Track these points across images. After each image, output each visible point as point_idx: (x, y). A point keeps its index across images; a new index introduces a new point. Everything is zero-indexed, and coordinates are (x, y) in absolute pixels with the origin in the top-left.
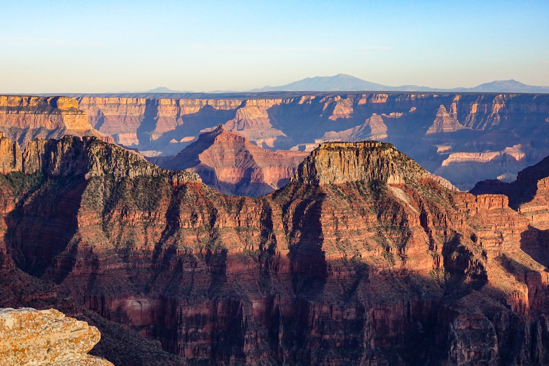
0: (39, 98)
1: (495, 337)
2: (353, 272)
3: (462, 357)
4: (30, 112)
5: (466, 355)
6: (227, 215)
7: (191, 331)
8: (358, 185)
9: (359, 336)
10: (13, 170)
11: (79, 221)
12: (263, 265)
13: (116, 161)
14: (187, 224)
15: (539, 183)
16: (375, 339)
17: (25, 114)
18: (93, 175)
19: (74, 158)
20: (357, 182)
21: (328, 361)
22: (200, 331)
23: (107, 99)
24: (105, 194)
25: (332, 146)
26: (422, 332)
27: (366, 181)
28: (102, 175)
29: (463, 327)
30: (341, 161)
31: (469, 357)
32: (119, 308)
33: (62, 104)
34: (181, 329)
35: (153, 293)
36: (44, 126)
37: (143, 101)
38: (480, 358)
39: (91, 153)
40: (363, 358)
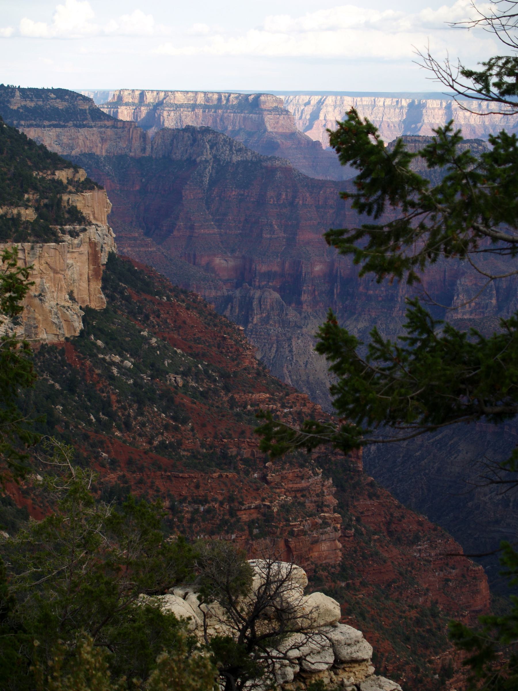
0: (240, 94)
1: (494, 292)
4: (229, 111)
6: (308, 195)
7: (263, 283)
11: (183, 194)
13: (222, 147)
14: (272, 200)
18: (203, 159)
19: (192, 145)
21: (369, 311)
22: (270, 284)
23: (359, 99)
24: (211, 174)
32: (208, 264)
33: (265, 102)
34: (255, 281)
35: (237, 254)
36: (243, 127)
37: (405, 103)
39: (203, 140)
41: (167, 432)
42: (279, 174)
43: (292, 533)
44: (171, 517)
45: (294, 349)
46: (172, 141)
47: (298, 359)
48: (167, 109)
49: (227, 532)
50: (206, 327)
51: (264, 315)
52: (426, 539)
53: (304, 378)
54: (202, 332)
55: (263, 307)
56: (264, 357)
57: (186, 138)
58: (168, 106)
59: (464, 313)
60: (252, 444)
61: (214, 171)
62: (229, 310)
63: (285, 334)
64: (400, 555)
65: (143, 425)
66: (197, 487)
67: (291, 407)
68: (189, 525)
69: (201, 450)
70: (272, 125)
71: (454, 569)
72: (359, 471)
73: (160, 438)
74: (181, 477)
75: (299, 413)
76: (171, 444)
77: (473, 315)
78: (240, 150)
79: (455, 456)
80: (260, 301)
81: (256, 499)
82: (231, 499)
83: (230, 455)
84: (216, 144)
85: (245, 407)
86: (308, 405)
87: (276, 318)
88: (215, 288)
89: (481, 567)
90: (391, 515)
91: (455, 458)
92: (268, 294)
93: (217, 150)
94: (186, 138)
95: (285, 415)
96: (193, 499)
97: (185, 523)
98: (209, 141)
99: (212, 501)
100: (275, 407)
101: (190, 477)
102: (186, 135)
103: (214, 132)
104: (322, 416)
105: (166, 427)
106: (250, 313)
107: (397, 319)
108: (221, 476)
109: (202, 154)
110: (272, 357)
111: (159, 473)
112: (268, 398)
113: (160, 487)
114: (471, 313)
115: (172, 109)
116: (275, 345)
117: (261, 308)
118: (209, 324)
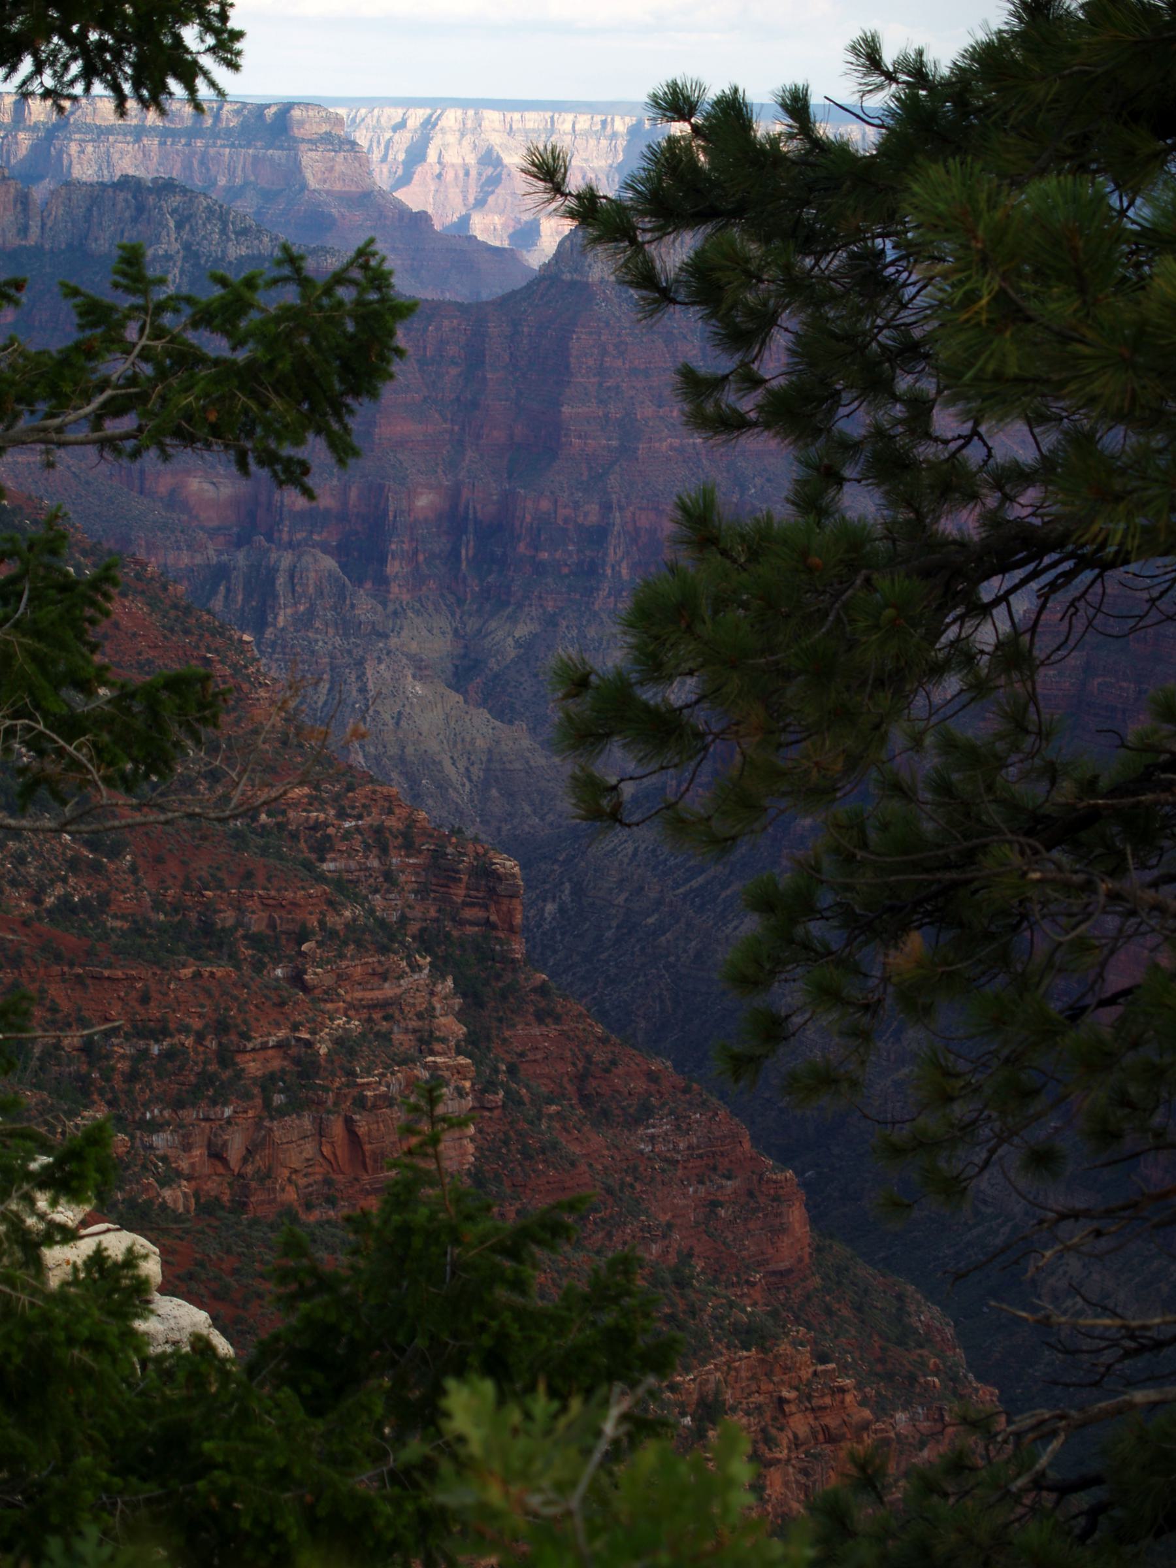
0: (244, 104)
2: (614, 443)
4: (219, 142)
7: (300, 536)
9: (600, 555)
10: (23, 243)
12: (456, 428)
13: (204, 224)
17: (207, 147)
18: (161, 252)
19: (135, 220)
21: (540, 598)
22: (316, 537)
23: (517, 116)
28: (178, 252)
32: (173, 492)
33: (302, 123)
34: (280, 531)
36: (252, 178)
37: (620, 125)
39: (161, 208)
40: (603, 594)
41: (75, 876)
43: (360, 1103)
44: (84, 1068)
45: (371, 686)
46: (89, 210)
48: (77, 136)
49: (214, 1102)
50: (165, 637)
51: (302, 608)
52: (666, 1111)
53: (393, 750)
54: (156, 647)
55: (298, 588)
57: (121, 205)
58: (79, 131)
60: (271, 902)
61: (185, 279)
63: (349, 652)
64: (608, 1148)
65: (20, 859)
66: (145, 999)
67: (360, 817)
68: (125, 1087)
69: (152, 916)
70: (319, 176)
71: (729, 1178)
72: (513, 961)
73: (59, 890)
74: (108, 978)
75: (378, 831)
76: (85, 904)
78: (245, 232)
79: (735, 923)
80: (292, 577)
81: (278, 1026)
82: (222, 1027)
83: (219, 926)
84: (189, 218)
85: (254, 818)
86: (397, 811)
87: (329, 615)
88: (189, 547)
89: (789, 1173)
90: (588, 1058)
91: (736, 928)
92: (310, 560)
93: (193, 231)
94: (121, 205)
95: (347, 835)
96: (134, 1027)
97: (118, 1083)
98: (173, 212)
99: (180, 1032)
100: (322, 816)
101: (128, 978)
102: (121, 196)
103: (184, 191)
104: (431, 836)
105: (74, 864)
107: (604, 616)
108: (198, 975)
109: (158, 240)
110: (320, 704)
111: (56, 969)
112: (307, 796)
113: (58, 1000)
115: (89, 137)
117: (293, 591)
118: (172, 630)
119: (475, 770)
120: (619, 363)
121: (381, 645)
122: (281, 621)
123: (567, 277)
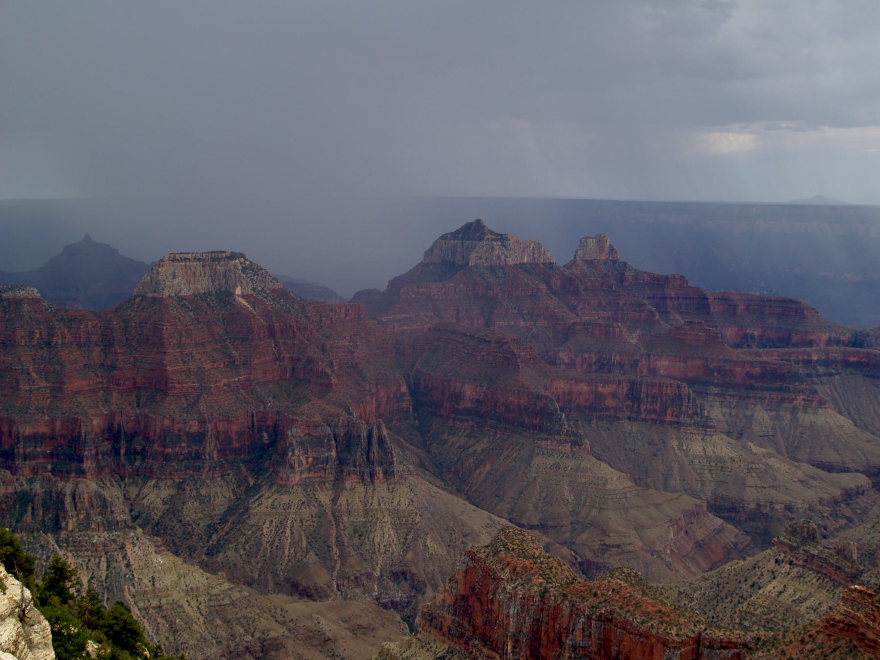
1: (333, 442)
3: (300, 463)
5: (304, 462)
6: (66, 331)
7: (29, 450)
8: (204, 297)
15: (402, 291)
16: (218, 451)
20: (204, 294)
25: (177, 257)
26: (267, 442)
27: (214, 293)
29: (302, 434)
30: (186, 272)
31: (307, 463)
38: (317, 464)
42: (26, 308)
45: (132, 562)
47: (141, 576)
51: (82, 517)
53: (155, 603)
55: (79, 505)
56: (92, 578)
59: (302, 473)
62: (30, 513)
63: (114, 541)
77: (312, 472)
80: (74, 498)
106: (61, 515)
107: (208, 481)
110: (104, 577)
114: (310, 471)
116: (103, 559)
117: (76, 507)
119: (202, 607)
120: (189, 340)
121: (132, 534)
122: (70, 527)
123: (150, 295)
